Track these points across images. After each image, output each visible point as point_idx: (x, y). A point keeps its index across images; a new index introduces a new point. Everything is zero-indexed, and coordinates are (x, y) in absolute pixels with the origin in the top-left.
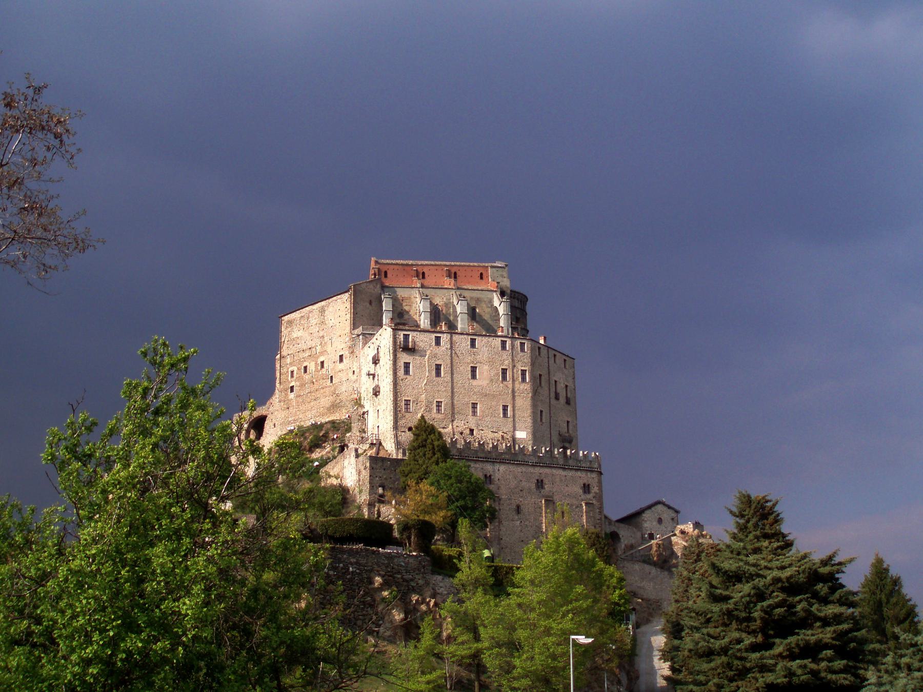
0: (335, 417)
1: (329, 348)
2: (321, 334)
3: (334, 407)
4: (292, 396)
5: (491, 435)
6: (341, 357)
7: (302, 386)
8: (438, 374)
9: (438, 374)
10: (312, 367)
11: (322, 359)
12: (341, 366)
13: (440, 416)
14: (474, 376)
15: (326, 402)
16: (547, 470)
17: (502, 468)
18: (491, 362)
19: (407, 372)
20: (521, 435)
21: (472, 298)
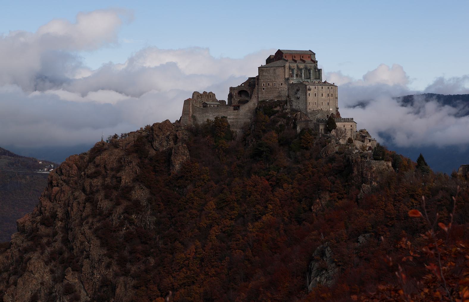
0: (280, 99)
1: (277, 81)
2: (274, 76)
3: (279, 96)
4: (264, 91)
5: (325, 110)
6: (282, 84)
7: (267, 89)
8: (315, 96)
9: (315, 96)
10: (271, 84)
11: (274, 83)
12: (281, 86)
13: (315, 106)
14: (322, 96)
15: (276, 94)
16: (345, 123)
17: (339, 123)
18: (326, 92)
19: (309, 96)
20: (331, 109)
21: (309, 66)
